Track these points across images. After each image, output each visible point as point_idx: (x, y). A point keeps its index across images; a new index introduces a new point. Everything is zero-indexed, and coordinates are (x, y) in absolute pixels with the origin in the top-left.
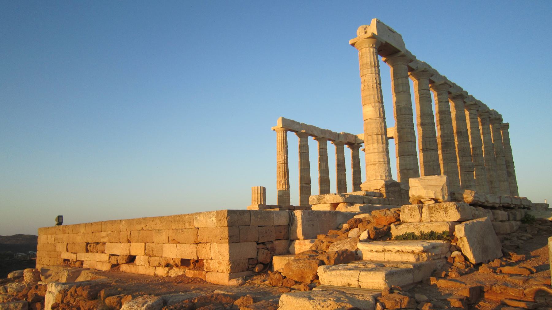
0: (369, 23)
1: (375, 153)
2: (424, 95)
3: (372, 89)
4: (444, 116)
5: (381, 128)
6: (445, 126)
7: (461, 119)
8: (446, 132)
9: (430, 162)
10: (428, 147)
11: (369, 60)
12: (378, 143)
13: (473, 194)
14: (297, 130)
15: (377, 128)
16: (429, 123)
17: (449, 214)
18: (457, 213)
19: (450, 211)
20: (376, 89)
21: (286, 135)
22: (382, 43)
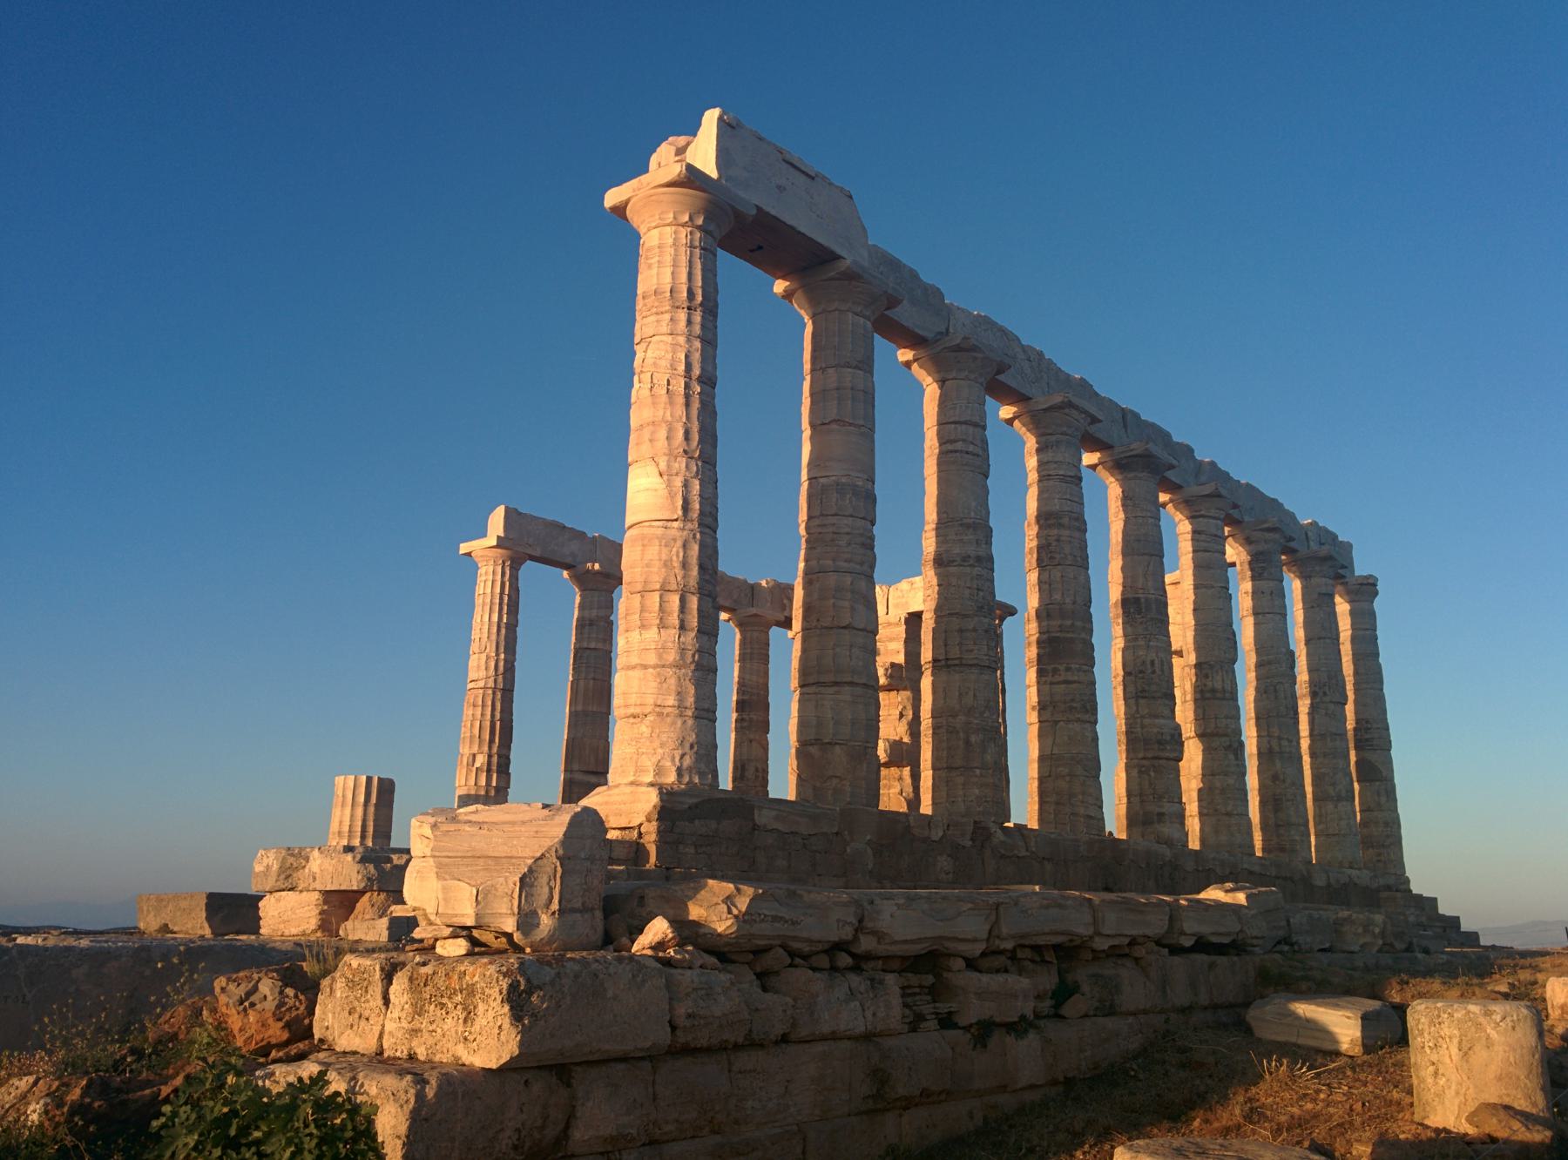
0: (692, 129)
1: (645, 667)
2: (959, 446)
3: (664, 398)
4: (1055, 532)
5: (685, 565)
6: (1057, 573)
7: (1145, 551)
8: (1057, 597)
9: (954, 716)
10: (955, 652)
11: (667, 279)
12: (662, 625)
13: (743, 904)
14: (569, 560)
15: (667, 564)
16: (965, 558)
17: (477, 1027)
18: (506, 1022)
19: (481, 1007)
20: (681, 400)
21: (514, 579)
22: (738, 215)
